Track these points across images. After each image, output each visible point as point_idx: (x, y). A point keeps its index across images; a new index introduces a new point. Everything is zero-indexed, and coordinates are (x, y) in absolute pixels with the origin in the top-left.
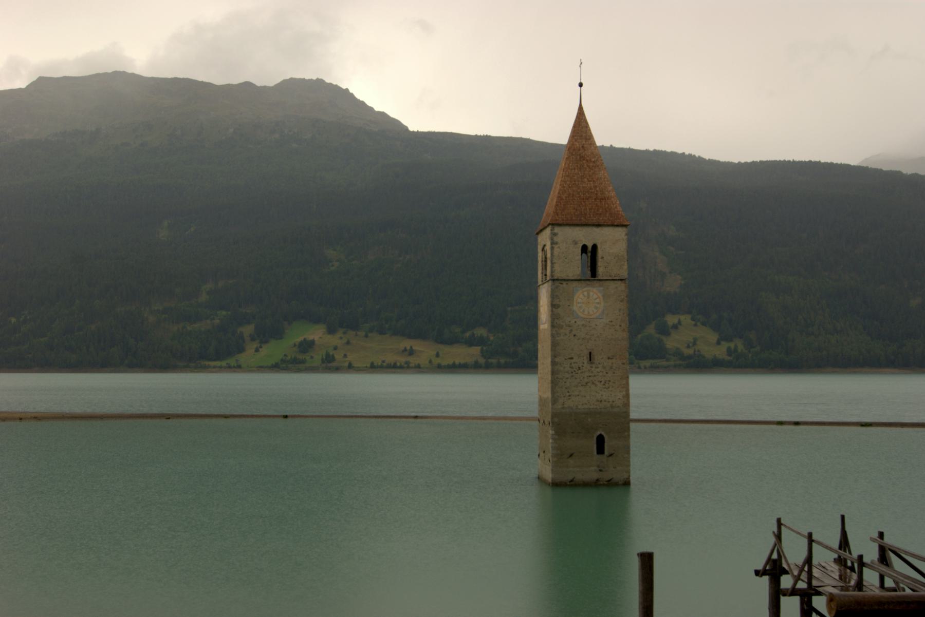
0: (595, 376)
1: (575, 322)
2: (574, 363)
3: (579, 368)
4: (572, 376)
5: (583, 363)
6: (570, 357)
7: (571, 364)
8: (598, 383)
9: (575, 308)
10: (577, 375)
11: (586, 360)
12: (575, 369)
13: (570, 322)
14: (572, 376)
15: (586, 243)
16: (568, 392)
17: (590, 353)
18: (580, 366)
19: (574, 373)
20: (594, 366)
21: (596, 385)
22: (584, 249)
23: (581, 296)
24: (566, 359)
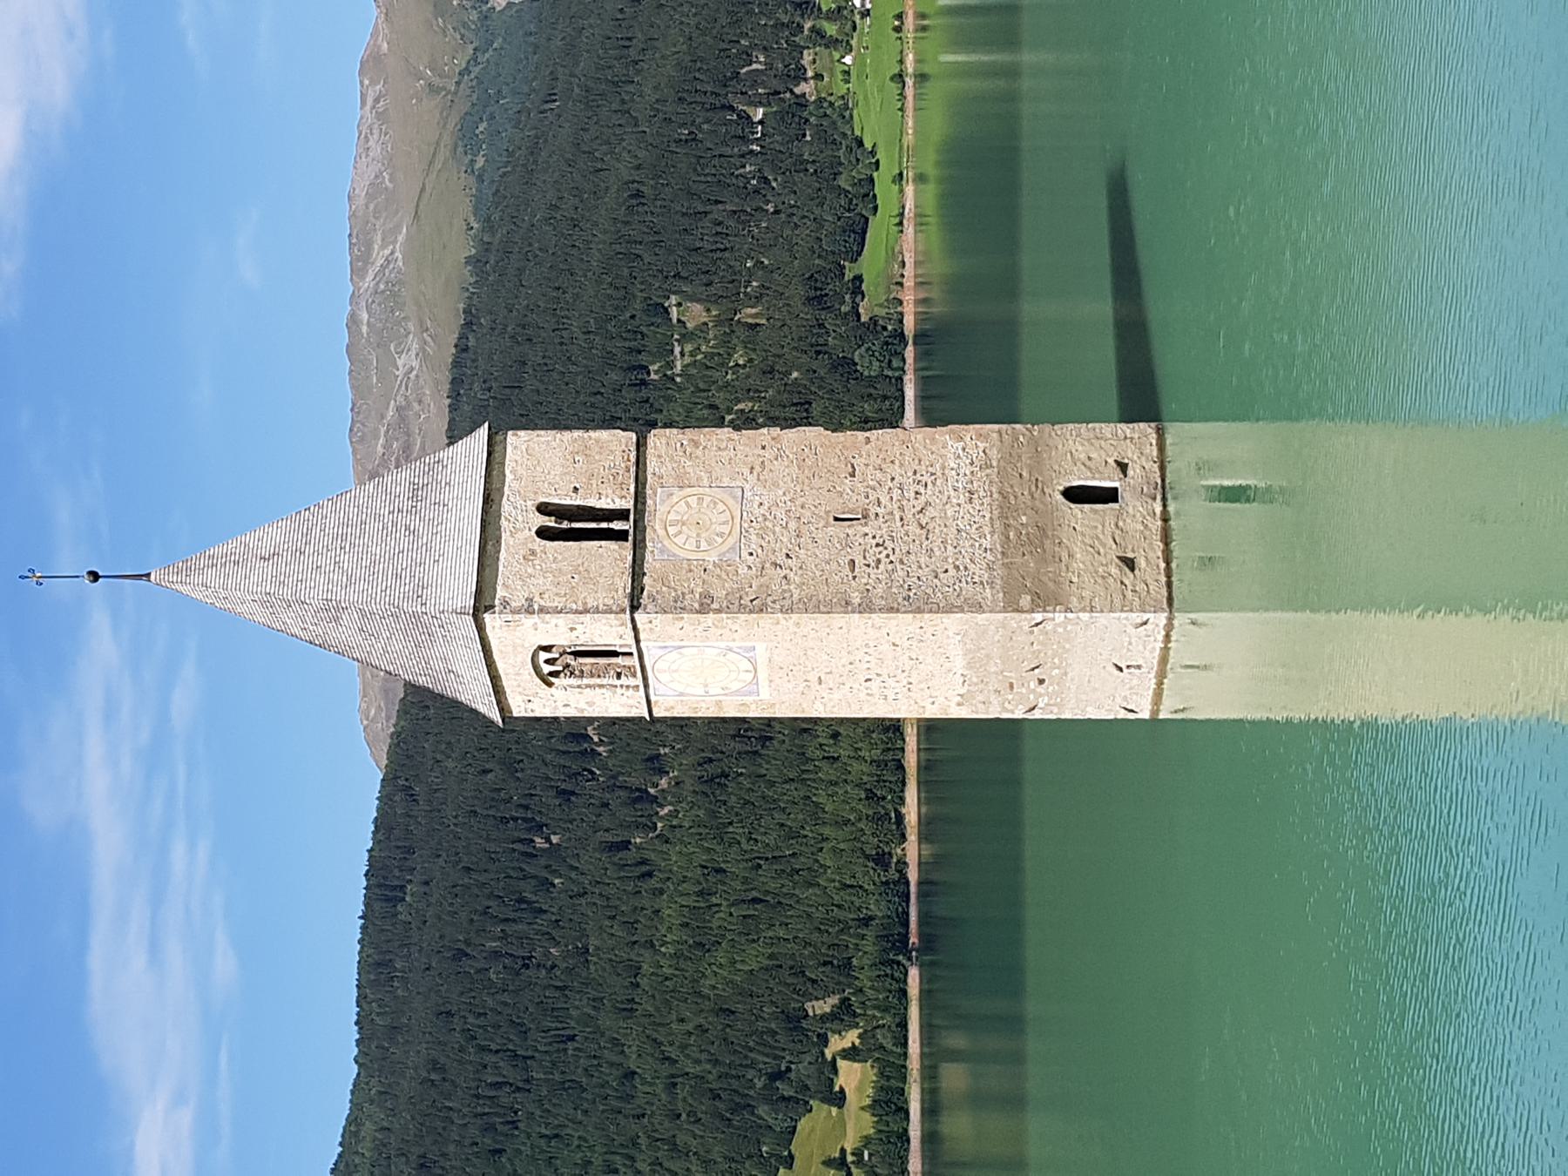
0: (901, 508)
1: (751, 554)
2: (865, 558)
3: (877, 545)
4: (902, 562)
5: (867, 534)
6: (847, 571)
7: (868, 566)
8: (922, 499)
9: (713, 557)
10: (897, 550)
11: (859, 528)
12: (882, 556)
13: (750, 567)
14: (902, 562)
15: (534, 529)
16: (946, 571)
17: (836, 519)
18: (874, 542)
19: (892, 558)
20: (873, 509)
21: (928, 504)
22: (543, 533)
23: (680, 540)
24: (854, 578)
